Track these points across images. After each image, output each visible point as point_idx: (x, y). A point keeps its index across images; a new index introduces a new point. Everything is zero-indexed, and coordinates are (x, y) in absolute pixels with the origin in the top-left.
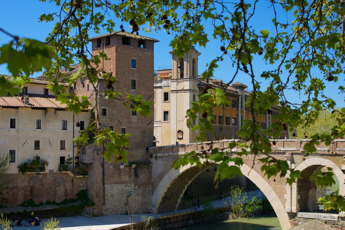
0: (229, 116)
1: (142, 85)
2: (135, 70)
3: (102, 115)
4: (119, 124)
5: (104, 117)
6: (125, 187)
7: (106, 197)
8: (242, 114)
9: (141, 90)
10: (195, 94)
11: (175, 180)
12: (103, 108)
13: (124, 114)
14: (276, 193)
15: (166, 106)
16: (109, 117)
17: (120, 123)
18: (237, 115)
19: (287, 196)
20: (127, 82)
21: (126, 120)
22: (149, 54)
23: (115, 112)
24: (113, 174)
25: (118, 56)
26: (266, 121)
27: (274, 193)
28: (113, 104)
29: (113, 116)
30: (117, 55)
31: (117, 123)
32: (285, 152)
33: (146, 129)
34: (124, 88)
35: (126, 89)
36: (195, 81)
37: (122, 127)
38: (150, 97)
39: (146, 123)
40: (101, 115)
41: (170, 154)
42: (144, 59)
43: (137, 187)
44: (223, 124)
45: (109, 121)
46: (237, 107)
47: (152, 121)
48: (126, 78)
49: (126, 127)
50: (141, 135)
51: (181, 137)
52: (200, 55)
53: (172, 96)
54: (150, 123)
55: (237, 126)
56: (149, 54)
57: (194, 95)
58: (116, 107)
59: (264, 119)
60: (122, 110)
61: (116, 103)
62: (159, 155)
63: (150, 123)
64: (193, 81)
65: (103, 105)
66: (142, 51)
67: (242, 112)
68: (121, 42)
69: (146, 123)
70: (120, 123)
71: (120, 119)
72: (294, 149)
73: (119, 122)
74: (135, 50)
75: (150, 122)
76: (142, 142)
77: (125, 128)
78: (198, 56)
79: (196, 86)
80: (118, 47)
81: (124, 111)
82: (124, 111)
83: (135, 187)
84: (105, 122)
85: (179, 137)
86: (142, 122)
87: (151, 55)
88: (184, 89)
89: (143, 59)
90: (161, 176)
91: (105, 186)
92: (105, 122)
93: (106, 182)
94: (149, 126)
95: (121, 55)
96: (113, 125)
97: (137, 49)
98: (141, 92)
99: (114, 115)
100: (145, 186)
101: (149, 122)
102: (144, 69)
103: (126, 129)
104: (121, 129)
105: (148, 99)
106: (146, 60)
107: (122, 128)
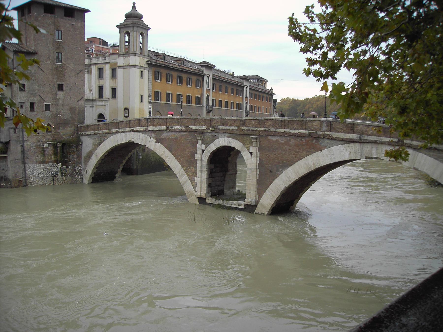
0: (190, 95)
2: (61, 42)
3: (20, 90)
4: (42, 101)
5: (23, 92)
6: (51, 166)
7: (28, 177)
8: (208, 94)
10: (142, 70)
11: (102, 160)
14: (188, 176)
15: (101, 83)
16: (28, 92)
18: (202, 95)
19: (197, 180)
21: (50, 96)
22: (79, 25)
24: (35, 153)
26: (242, 102)
27: (186, 175)
28: (33, 78)
32: (196, 130)
34: (47, 61)
35: (49, 62)
36: (143, 56)
37: (45, 104)
38: (80, 72)
41: (96, 131)
43: (65, 166)
44: (172, 102)
46: (202, 86)
47: (83, 97)
49: (50, 104)
50: (69, 112)
51: (127, 115)
52: (151, 30)
53: (120, 72)
54: (80, 99)
55: (201, 106)
59: (241, 99)
62: (87, 133)
63: (80, 99)
66: (70, 22)
67: (208, 90)
68: (42, 11)
69: (76, 99)
71: (42, 95)
72: (204, 127)
73: (42, 98)
76: (70, 120)
77: (49, 105)
78: (149, 31)
81: (47, 86)
82: (47, 86)
83: (62, 165)
84: (24, 97)
85: (126, 115)
86: (70, 97)
87: (81, 26)
88: (131, 64)
89: (71, 30)
90: (90, 155)
91: (26, 165)
92: (24, 97)
93: (27, 161)
96: (34, 102)
97: (63, 19)
98: (69, 66)
99: (34, 90)
100: (75, 165)
101: (80, 98)
102: (73, 41)
103: (50, 106)
105: (78, 74)
106: (75, 31)
107: (45, 105)
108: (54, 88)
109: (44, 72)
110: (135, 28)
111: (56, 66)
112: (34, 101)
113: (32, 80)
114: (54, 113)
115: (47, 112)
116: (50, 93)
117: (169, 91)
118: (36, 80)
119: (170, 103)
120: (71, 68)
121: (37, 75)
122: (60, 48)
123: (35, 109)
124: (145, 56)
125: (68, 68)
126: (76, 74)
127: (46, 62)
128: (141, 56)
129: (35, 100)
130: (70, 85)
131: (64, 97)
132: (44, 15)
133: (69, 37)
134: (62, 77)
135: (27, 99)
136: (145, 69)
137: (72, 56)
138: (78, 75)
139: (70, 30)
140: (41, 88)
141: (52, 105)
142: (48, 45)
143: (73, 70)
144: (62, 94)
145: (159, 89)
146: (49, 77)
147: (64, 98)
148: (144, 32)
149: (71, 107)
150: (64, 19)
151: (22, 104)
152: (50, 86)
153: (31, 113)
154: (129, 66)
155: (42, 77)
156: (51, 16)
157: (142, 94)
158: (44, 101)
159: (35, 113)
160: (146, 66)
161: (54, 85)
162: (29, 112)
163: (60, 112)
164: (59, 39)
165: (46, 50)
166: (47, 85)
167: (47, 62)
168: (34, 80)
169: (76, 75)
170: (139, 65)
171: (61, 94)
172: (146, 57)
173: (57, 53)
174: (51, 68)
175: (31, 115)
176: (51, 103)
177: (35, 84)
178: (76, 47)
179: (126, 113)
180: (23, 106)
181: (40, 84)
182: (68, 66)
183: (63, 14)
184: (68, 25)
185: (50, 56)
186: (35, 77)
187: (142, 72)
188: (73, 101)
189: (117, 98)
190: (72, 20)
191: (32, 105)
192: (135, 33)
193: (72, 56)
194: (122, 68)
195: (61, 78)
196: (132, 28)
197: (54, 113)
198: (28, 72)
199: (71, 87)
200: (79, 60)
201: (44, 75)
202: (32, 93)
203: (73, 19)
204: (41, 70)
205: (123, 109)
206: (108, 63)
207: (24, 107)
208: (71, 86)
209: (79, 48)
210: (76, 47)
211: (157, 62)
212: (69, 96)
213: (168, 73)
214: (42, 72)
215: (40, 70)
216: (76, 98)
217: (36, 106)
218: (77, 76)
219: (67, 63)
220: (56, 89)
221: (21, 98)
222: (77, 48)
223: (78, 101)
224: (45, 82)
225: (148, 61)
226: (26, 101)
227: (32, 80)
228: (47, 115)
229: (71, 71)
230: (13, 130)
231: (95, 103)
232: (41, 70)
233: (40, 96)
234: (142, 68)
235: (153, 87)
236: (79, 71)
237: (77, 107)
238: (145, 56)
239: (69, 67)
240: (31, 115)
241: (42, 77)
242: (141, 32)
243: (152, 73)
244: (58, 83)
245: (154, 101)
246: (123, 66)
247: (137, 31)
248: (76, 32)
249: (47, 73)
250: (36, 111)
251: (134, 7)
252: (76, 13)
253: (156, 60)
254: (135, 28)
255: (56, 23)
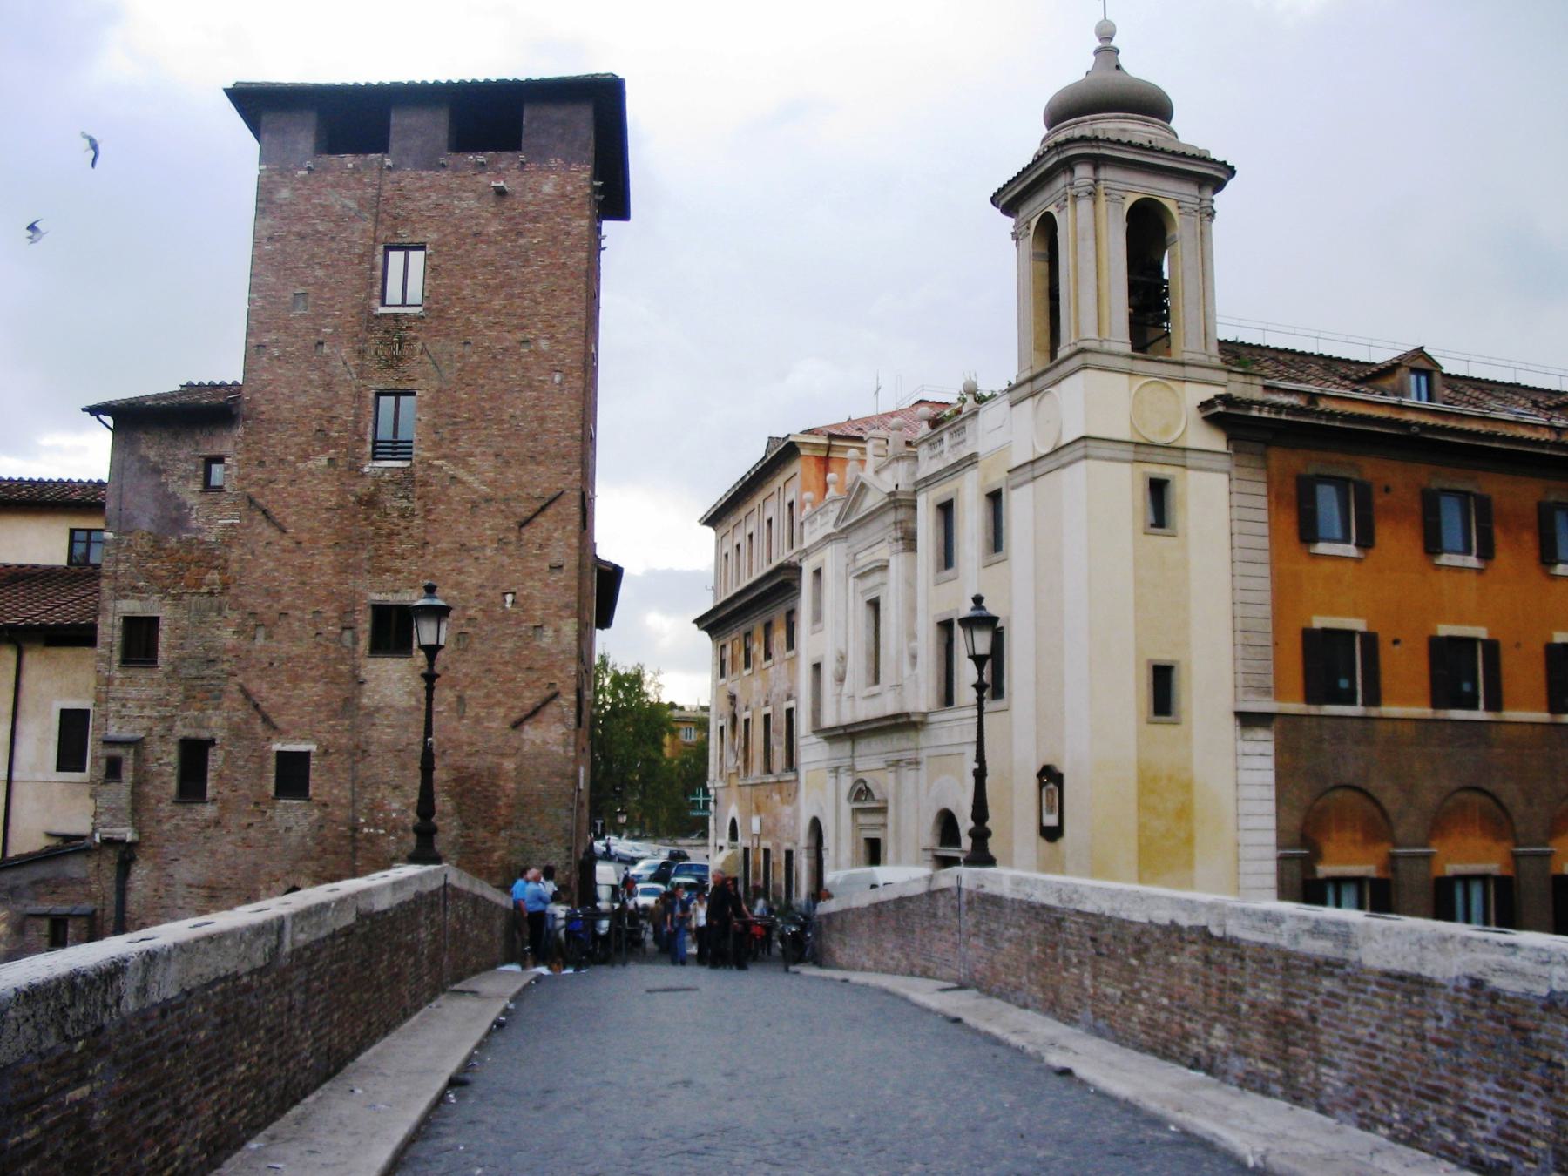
1: (469, 420)
4: (259, 726)
5: (142, 675)
9: (461, 460)
12: (131, 607)
13: (296, 650)
16: (175, 671)
17: (266, 719)
20: (339, 410)
21: (312, 690)
23: (227, 636)
25: (270, 238)
28: (214, 576)
29: (211, 662)
30: (264, 233)
31: (239, 715)
33: (496, 760)
34: (305, 457)
35: (323, 461)
37: (277, 746)
38: (543, 509)
39: (500, 711)
40: (117, 657)
42: (497, 232)
45: (175, 699)
47: (556, 695)
48: (328, 386)
49: (313, 747)
54: (535, 712)
56: (547, 188)
57: (1158, 489)
58: (236, 596)
60: (283, 614)
61: (235, 567)
63: (535, 712)
64: (1130, 373)
65: (134, 588)
66: (482, 179)
69: (500, 711)
70: (266, 719)
71: (259, 687)
73: (256, 706)
74: (421, 179)
75: (537, 701)
77: (307, 754)
79: (1195, 416)
80: (277, 178)
81: (296, 625)
86: (461, 699)
87: (563, 196)
89: (491, 230)
92: (143, 707)
94: (531, 733)
95: (297, 228)
96: (205, 735)
98: (461, 473)
99: (212, 655)
101: (530, 699)
102: (497, 304)
103: (314, 762)
104: (273, 762)
106: (520, 234)
107: (281, 755)
108: (348, 634)
109: (284, 531)
110: (1083, 172)
111: (369, 481)
112: (208, 728)
113: (204, 590)
114: (339, 814)
115: (287, 808)
116: (314, 673)
117: (1459, 620)
118: (226, 586)
119: (1480, 715)
120: (476, 485)
121: (236, 552)
122: (400, 359)
123: (210, 793)
124: (1183, 364)
125: (452, 491)
126: (508, 529)
127: (300, 466)
128: (1140, 366)
129: (215, 724)
130: (464, 608)
131: (410, 693)
132: (308, 163)
133: (474, 277)
134: (403, 558)
135: (164, 718)
136: (1191, 459)
137: (487, 405)
138: (527, 533)
139: (476, 235)
140: (260, 641)
141: (326, 752)
142: (326, 349)
143: (488, 500)
144: (401, 679)
145: (1357, 615)
146: (318, 560)
147: (413, 703)
148: (1169, 193)
149: (458, 769)
150: (443, 166)
151: (118, 751)
152: (315, 626)
153: (179, 809)
154: (1060, 454)
155: (271, 565)
156: (355, 168)
157: (1164, 657)
158: (275, 728)
159: (209, 811)
160: (1216, 441)
161: (346, 612)
162: (166, 807)
163: (374, 807)
164: (404, 304)
165: (310, 381)
166: (298, 613)
167: (310, 464)
168: (217, 589)
169: (512, 537)
170: (1126, 436)
171: (396, 676)
172: (1191, 372)
173: (379, 394)
174: (334, 500)
175: (177, 827)
176: (320, 744)
177: (219, 610)
178: (520, 335)
179: (1051, 811)
180: (124, 766)
181: (253, 614)
182: (453, 478)
183: (442, 135)
184: (469, 202)
185: (331, 420)
186: (223, 569)
187: (1158, 489)
188: (478, 720)
189: (1010, 694)
190: (501, 166)
191: (194, 754)
192: (1085, 206)
193: (487, 405)
194: (1027, 473)
195: (398, 564)
196: (1061, 181)
197: (339, 814)
198: (179, 540)
199: (471, 620)
200: (535, 424)
201: (284, 551)
202: (193, 672)
203: (505, 159)
204: (264, 512)
205: (1035, 769)
206: (972, 459)
207: (128, 775)
208: (471, 612)
209: (544, 345)
210: (520, 335)
211: (1323, 405)
212: (453, 687)
213: (1436, 484)
214: (270, 532)
215: (259, 516)
216: (499, 703)
217: (216, 760)
218: (519, 539)
219: (444, 457)
220: (356, 641)
221: (124, 712)
222: (527, 342)
223: (517, 725)
224: (288, 599)
225: (1227, 400)
226: (158, 730)
227: (204, 590)
228: (288, 829)
229: (475, 505)
230: (46, 923)
231: (923, 739)
232: (264, 512)
233: (246, 694)
234: (1158, 455)
235: (1284, 593)
236: (538, 505)
237: (509, 765)
238: (1183, 364)
239: (463, 483)
240: (177, 827)
241: (271, 565)
242: (1132, 199)
243: (1262, 489)
244: (377, 597)
245: (1296, 707)
246: (1033, 462)
247: (1093, 194)
248: (522, 241)
249: (306, 536)
250: (214, 800)
251: (1107, 52)
252: (529, 115)
253: (1312, 398)
254: (1083, 172)
255: (387, 200)
